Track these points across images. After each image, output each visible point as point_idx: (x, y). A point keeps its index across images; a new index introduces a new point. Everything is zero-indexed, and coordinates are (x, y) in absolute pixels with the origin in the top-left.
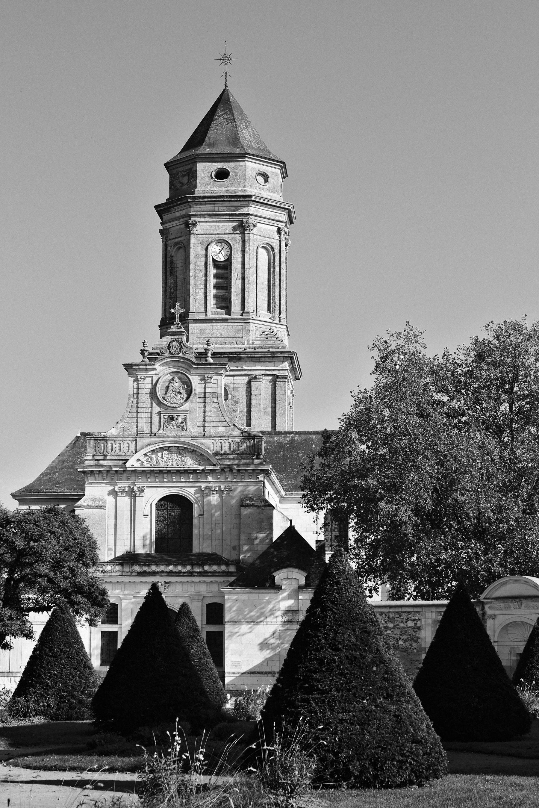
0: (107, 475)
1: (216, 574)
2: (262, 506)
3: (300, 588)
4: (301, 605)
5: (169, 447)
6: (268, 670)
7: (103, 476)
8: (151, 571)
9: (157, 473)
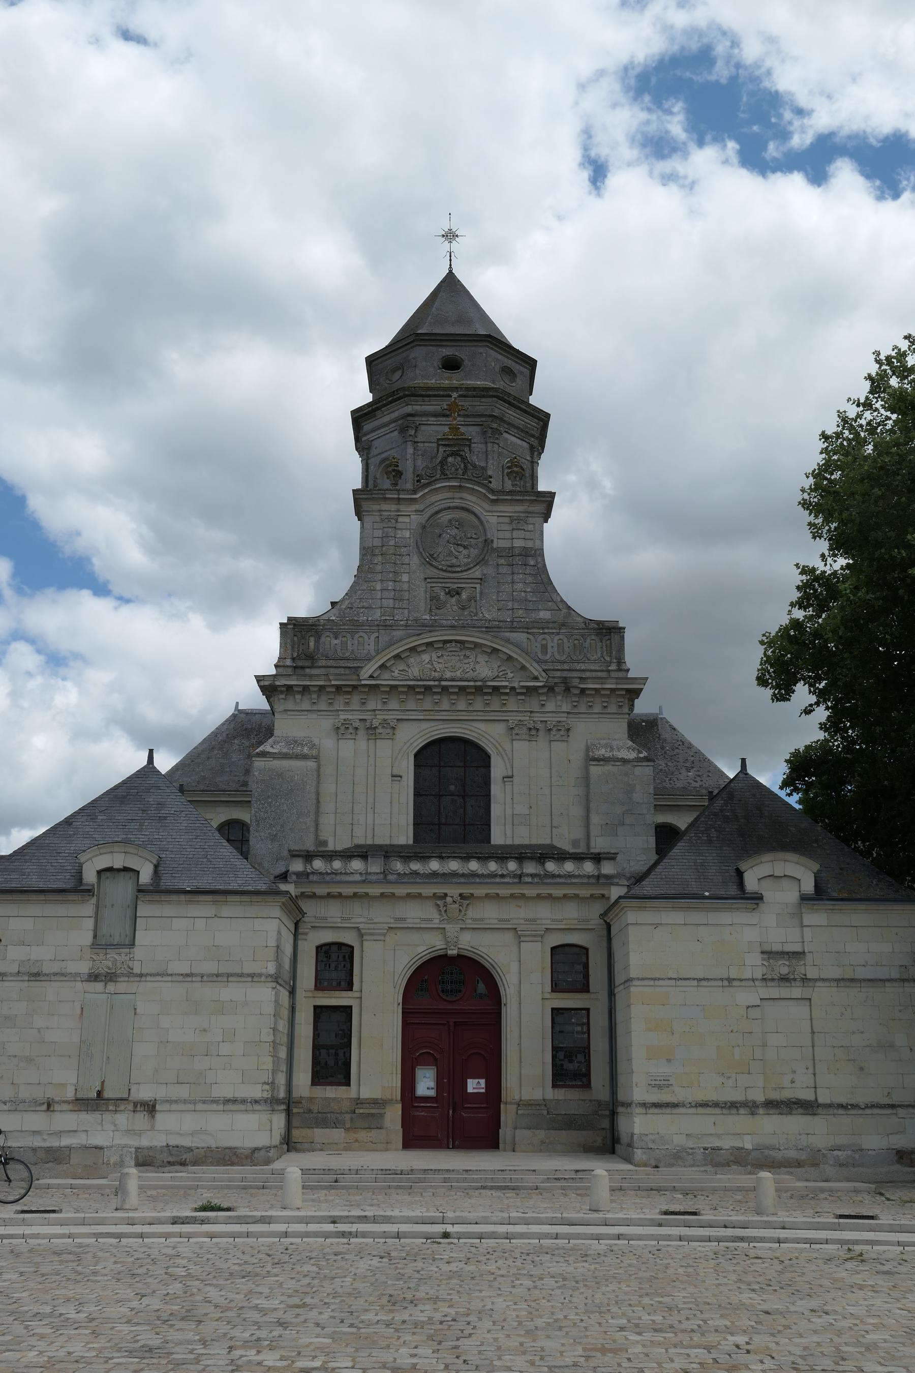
0: (319, 696)
1: (574, 881)
2: (633, 760)
3: (804, 898)
4: (807, 938)
5: (445, 642)
6: (738, 1096)
7: (311, 699)
8: (427, 871)
9: (419, 693)
